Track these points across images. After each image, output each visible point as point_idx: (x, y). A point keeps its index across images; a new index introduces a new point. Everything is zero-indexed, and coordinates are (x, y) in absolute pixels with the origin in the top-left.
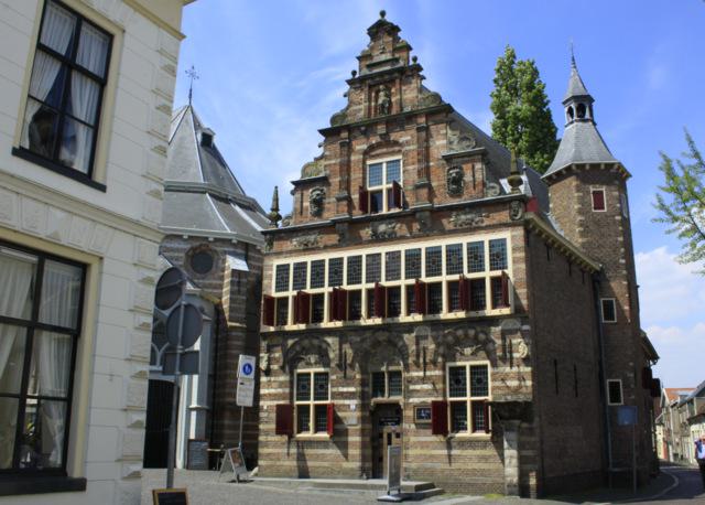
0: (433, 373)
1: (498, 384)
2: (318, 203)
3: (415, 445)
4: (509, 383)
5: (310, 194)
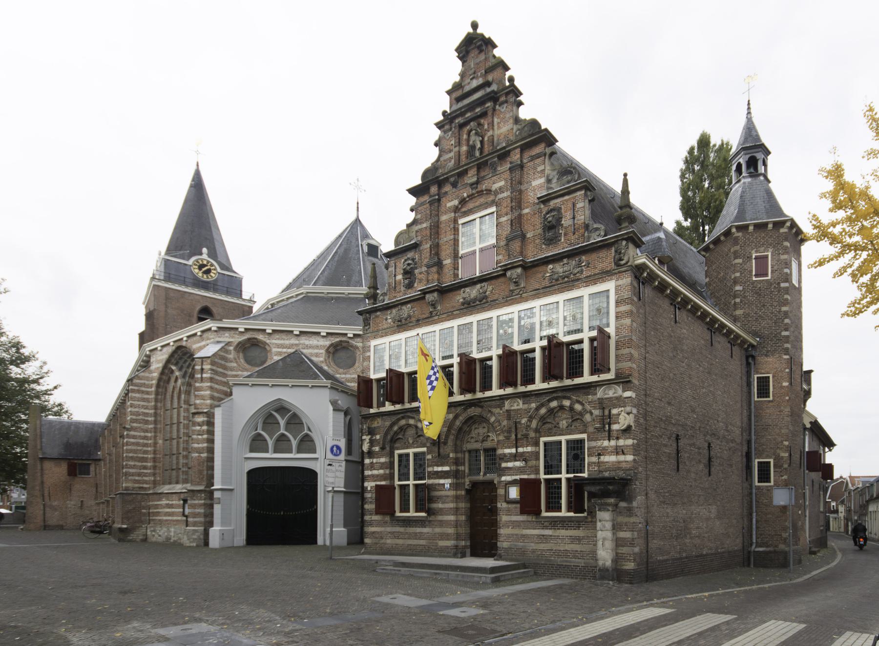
0: (525, 449)
1: (594, 459)
3: (507, 524)
4: (606, 458)
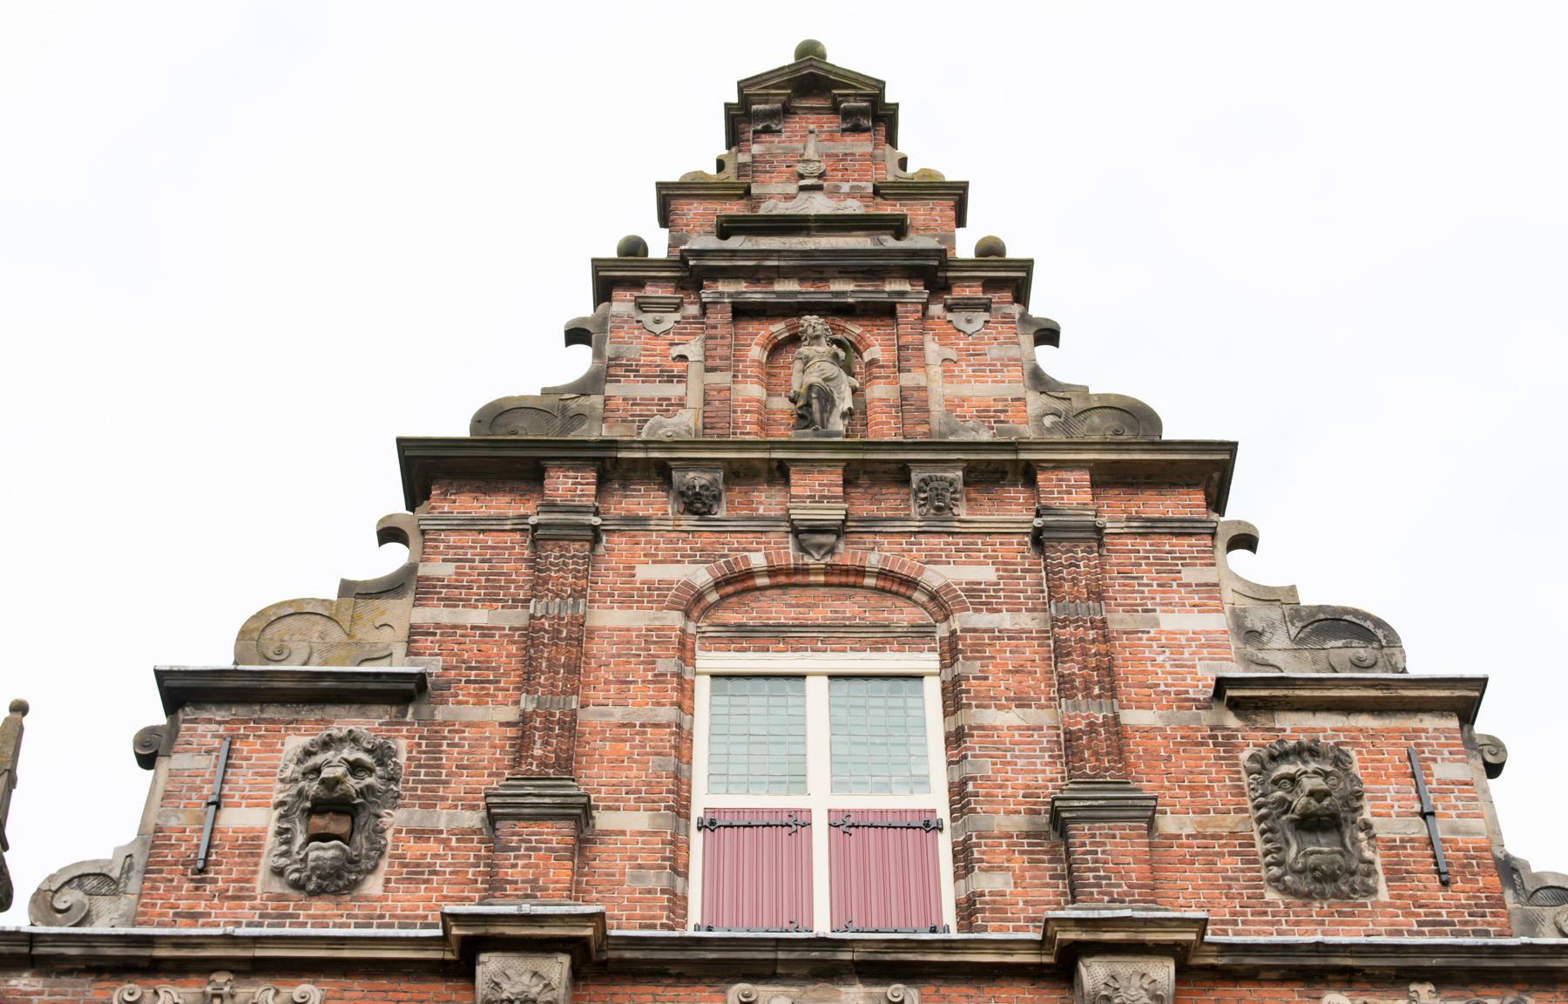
2: (335, 809)
5: (284, 747)
